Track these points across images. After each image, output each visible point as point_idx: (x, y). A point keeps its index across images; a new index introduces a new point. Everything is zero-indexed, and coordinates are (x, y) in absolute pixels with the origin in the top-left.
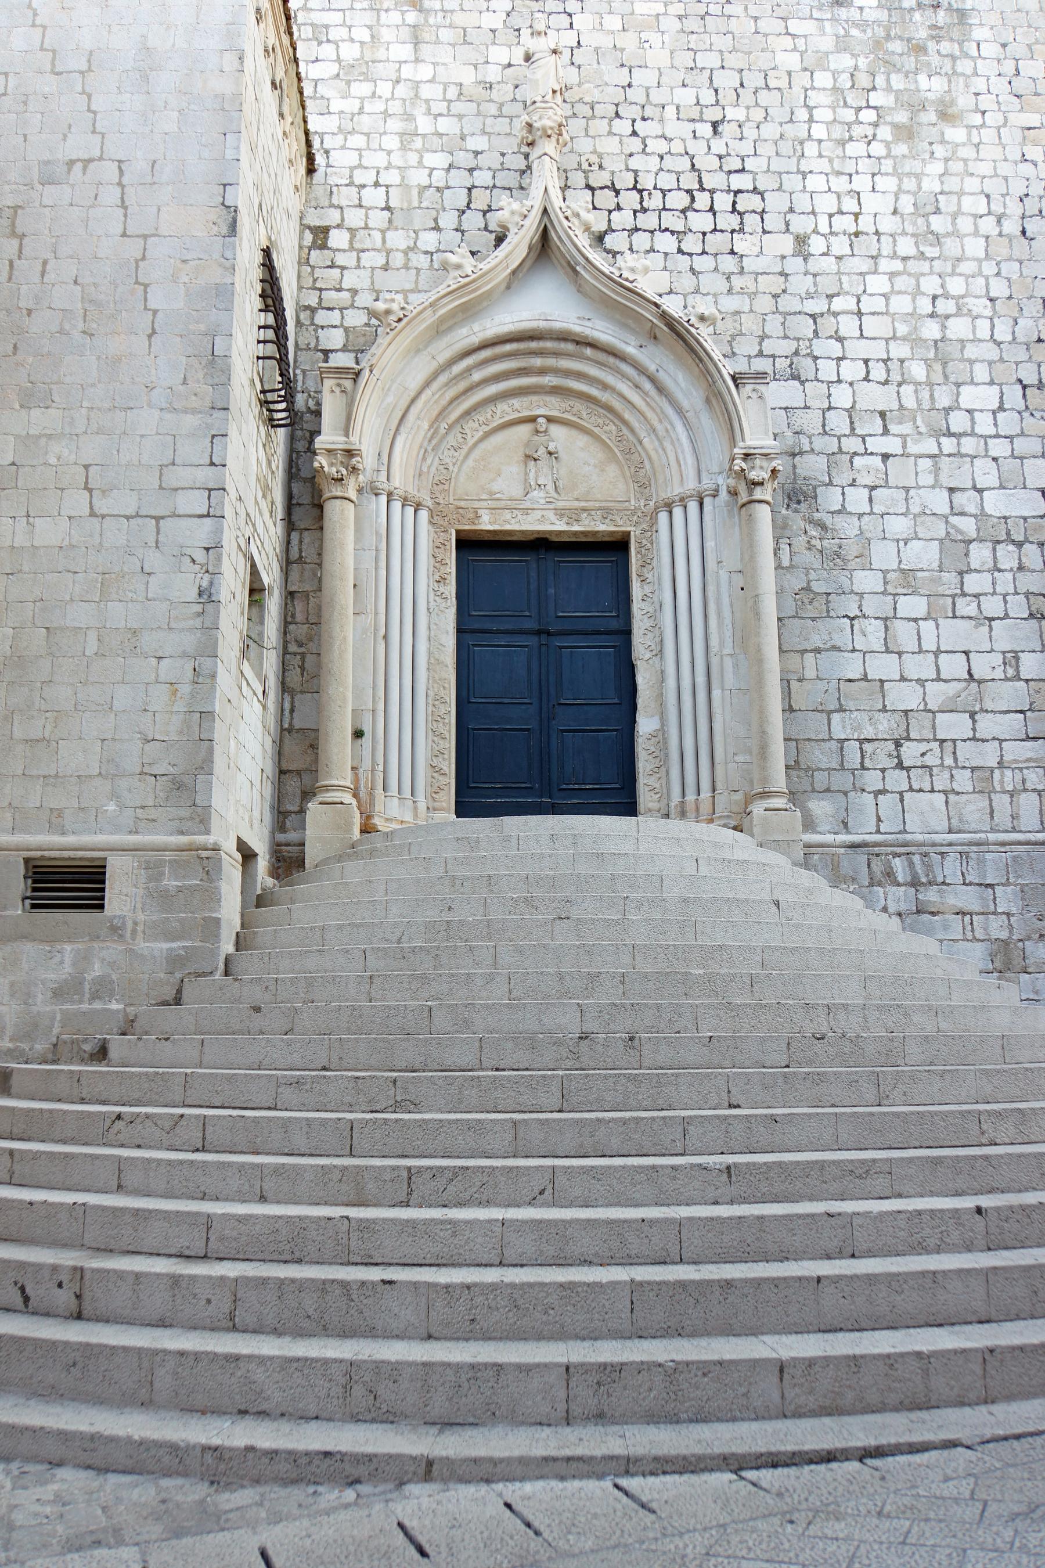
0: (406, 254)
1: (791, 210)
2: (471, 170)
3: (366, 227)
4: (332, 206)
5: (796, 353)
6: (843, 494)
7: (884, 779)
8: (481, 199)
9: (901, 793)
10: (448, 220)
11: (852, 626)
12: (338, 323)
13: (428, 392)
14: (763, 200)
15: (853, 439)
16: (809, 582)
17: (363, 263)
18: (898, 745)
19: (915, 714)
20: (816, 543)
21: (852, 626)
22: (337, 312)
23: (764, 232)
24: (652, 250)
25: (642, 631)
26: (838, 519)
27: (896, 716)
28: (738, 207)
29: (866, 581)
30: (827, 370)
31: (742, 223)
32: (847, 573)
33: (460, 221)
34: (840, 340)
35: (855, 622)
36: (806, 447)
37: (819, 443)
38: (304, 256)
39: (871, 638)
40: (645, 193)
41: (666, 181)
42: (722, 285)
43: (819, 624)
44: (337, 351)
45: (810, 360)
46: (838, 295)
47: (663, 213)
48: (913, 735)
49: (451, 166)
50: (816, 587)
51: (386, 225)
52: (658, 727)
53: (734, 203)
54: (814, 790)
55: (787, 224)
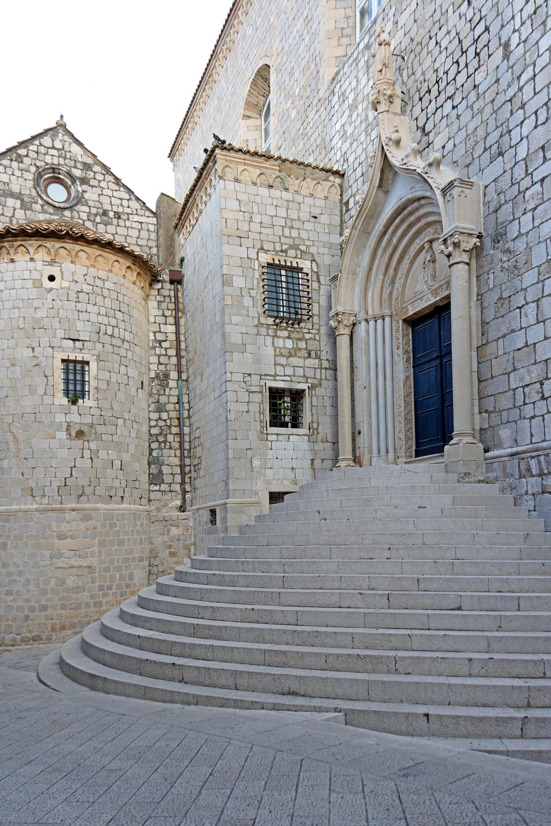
13: (377, 262)
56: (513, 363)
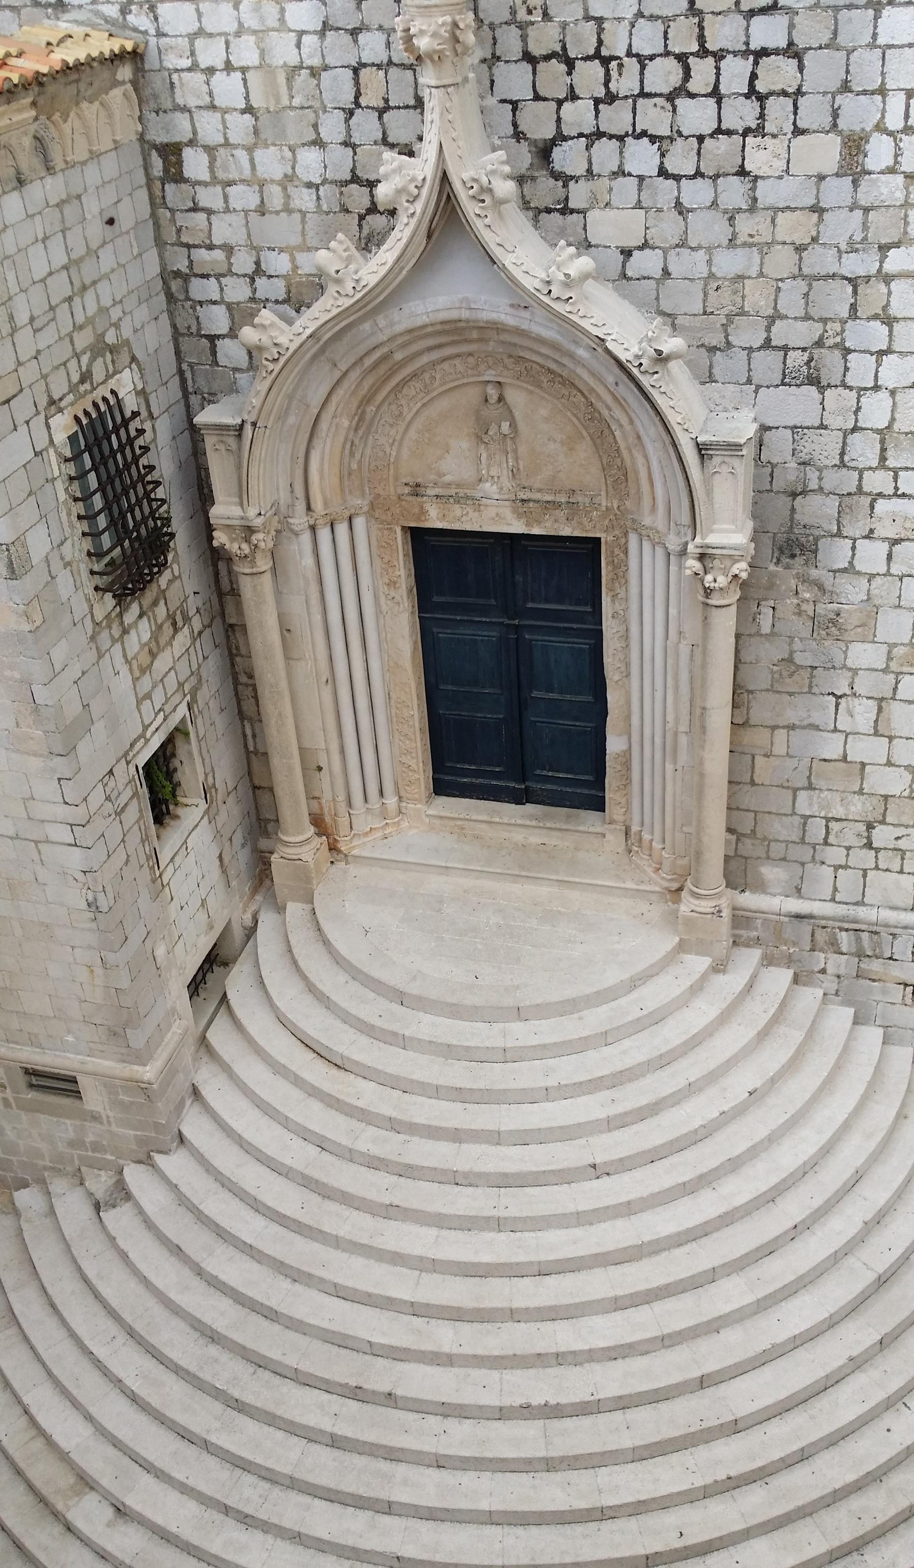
0: (285, 189)
1: (846, 87)
2: (354, 33)
3: (227, 144)
4: (178, 108)
5: (819, 343)
6: (853, 548)
7: (848, 855)
8: (374, 87)
9: (865, 871)
10: (332, 127)
11: (837, 705)
12: (216, 296)
14: (801, 68)
15: (881, 474)
16: (792, 653)
17: (233, 204)
18: (870, 826)
19: (897, 801)
20: (809, 608)
21: (837, 705)
22: (213, 280)
23: (798, 132)
24: (621, 172)
25: (611, 652)
26: (842, 579)
27: (875, 800)
28: (761, 87)
29: (864, 655)
30: (861, 369)
31: (762, 116)
32: (842, 645)
33: (348, 129)
34: (889, 321)
35: (843, 701)
36: (813, 485)
37: (832, 479)
38: (158, 193)
39: (858, 718)
40: (614, 64)
41: (647, 39)
42: (720, 230)
43: (798, 699)
44: (223, 337)
45: (837, 353)
46: (897, 245)
47: (641, 102)
48: (888, 820)
49: (326, 27)
50: (799, 659)
51: (251, 140)
52: (625, 747)
53: (754, 76)
54: (768, 858)
55: (835, 114)
56: (809, 777)
